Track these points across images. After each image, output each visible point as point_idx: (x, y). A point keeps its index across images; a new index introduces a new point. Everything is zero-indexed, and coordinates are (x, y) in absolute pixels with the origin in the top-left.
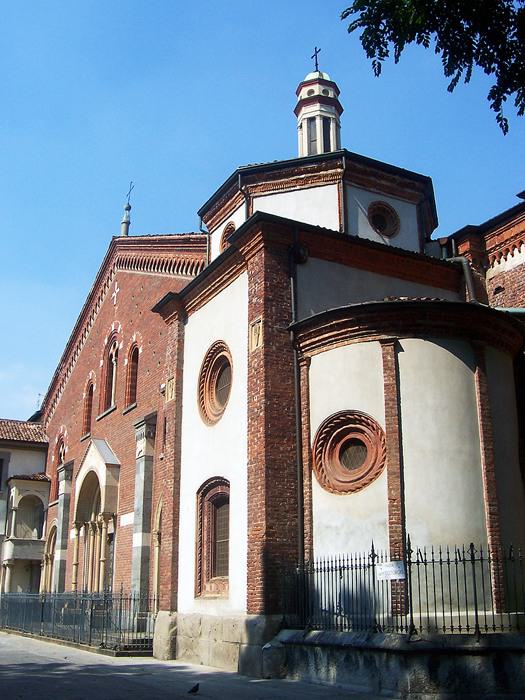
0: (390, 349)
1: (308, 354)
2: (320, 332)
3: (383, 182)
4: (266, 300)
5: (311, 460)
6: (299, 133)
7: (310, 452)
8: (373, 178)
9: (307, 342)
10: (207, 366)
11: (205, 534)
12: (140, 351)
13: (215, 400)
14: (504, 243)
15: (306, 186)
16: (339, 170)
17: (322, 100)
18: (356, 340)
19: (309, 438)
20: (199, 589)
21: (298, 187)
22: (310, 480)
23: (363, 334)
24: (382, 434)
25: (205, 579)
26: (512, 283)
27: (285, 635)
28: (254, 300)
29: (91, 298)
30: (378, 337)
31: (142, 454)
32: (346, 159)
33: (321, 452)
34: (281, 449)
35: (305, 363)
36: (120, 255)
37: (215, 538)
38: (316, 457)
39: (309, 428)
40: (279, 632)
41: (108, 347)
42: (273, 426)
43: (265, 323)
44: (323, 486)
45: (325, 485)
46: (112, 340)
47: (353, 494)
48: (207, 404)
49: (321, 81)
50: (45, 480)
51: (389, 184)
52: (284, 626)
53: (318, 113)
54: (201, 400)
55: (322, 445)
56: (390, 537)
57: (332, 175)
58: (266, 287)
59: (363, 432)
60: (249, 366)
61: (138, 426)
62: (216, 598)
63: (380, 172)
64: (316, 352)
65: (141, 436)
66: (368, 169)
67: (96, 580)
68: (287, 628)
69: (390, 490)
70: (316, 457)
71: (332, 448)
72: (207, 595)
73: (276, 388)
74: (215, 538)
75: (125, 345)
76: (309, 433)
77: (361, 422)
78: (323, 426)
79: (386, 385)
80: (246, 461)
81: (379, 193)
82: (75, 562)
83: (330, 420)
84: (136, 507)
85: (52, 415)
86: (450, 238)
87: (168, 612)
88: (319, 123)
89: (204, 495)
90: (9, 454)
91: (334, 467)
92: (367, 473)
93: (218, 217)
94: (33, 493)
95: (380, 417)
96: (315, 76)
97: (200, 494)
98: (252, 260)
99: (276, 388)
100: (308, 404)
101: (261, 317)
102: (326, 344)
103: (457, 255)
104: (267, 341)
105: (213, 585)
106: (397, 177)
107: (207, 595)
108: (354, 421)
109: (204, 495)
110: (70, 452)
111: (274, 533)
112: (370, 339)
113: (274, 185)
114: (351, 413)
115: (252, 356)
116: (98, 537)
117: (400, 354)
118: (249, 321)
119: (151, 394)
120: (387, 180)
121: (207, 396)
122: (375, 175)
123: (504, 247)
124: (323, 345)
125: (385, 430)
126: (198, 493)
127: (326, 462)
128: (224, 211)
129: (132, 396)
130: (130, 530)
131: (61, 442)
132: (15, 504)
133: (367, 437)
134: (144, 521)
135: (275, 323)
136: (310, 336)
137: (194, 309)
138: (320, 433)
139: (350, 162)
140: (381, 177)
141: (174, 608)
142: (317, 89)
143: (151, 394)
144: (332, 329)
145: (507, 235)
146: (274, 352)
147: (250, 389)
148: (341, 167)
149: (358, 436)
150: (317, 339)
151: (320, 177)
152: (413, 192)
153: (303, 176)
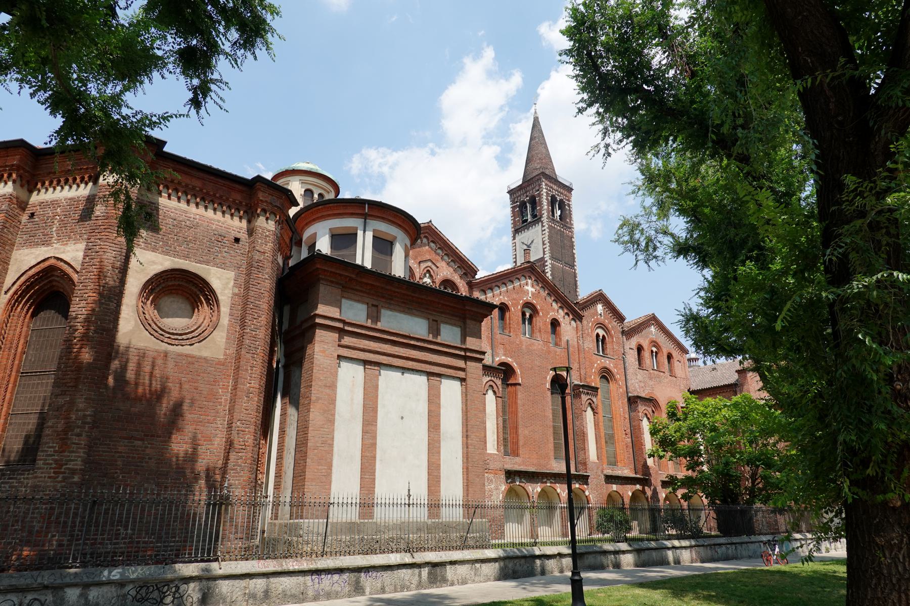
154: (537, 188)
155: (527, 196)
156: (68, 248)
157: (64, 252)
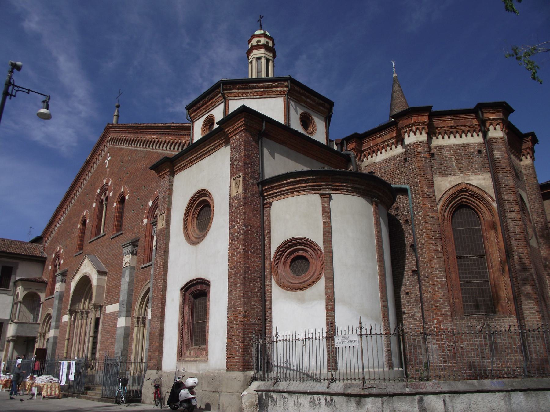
0: (326, 200)
1: (270, 200)
2: (281, 186)
3: (308, 100)
4: (245, 163)
5: (271, 268)
6: (250, 66)
7: (271, 263)
8: (303, 97)
9: (271, 192)
10: (191, 206)
11: (186, 317)
12: (127, 198)
13: (196, 228)
14: (376, 145)
15: (264, 96)
16: (285, 89)
17: (266, 47)
18: (305, 193)
19: (270, 254)
20: (181, 355)
21: (258, 97)
22: (271, 282)
23: (310, 190)
24: (321, 252)
25: (185, 348)
26: (380, 169)
27: (255, 385)
28: (236, 163)
29: (88, 163)
30: (319, 192)
31: (127, 265)
32: (290, 82)
33: (277, 263)
34: (253, 260)
35: (268, 205)
36: (111, 136)
37: (193, 319)
38: (275, 266)
39: (270, 248)
40: (251, 383)
41: (100, 195)
42: (248, 245)
43: (244, 178)
44: (280, 285)
45: (282, 285)
46: (104, 190)
47: (302, 292)
48: (190, 231)
49: (265, 35)
50: (43, 282)
51: (311, 102)
52: (254, 379)
53: (263, 55)
54: (186, 228)
55: (279, 259)
56: (327, 319)
57: (281, 91)
58: (245, 155)
59: (306, 251)
60: (230, 205)
61: (125, 246)
62: (196, 361)
63: (307, 94)
64: (276, 199)
65: (127, 253)
66: (301, 91)
67: (82, 350)
68: (256, 380)
69: (326, 288)
70: (275, 266)
71: (286, 261)
72: (187, 359)
73: (250, 220)
74: (193, 319)
75: (114, 194)
76: (270, 252)
77: (306, 245)
78: (281, 247)
79: (324, 222)
80: (227, 268)
81: (306, 107)
82: (67, 337)
83: (285, 243)
84: (121, 299)
85: (50, 238)
86: (343, 140)
87: (155, 371)
88: (263, 61)
89: (186, 291)
90: (17, 265)
91: (285, 271)
92: (310, 278)
93: (200, 111)
94: (33, 290)
95: (320, 242)
96: (261, 32)
97: (183, 290)
98: (234, 137)
99: (250, 220)
100: (270, 232)
101: (242, 174)
102: (283, 194)
103: (346, 150)
104: (245, 189)
105: (192, 352)
106: (316, 99)
107: (187, 359)
108: (301, 244)
109: (186, 291)
110: (64, 263)
111: (248, 316)
112: (314, 192)
113: (243, 93)
114: (301, 239)
115: (233, 199)
116: (85, 321)
117: (332, 202)
118: (231, 176)
119: (134, 226)
120: (310, 99)
121: (190, 226)
122: (305, 96)
123: (375, 148)
124: (282, 195)
125: (323, 251)
126: (182, 289)
127: (281, 270)
128: (206, 107)
129: (119, 227)
130: (115, 316)
131: (57, 257)
132: (20, 298)
133: (310, 254)
134: (127, 310)
135: (250, 179)
136: (273, 188)
137: (181, 169)
138: (278, 251)
139: (292, 84)
140: (308, 97)
141: (159, 367)
142: (263, 40)
143: (134, 226)
144: (289, 184)
145: (379, 140)
146: (249, 197)
147: (231, 221)
148: (287, 86)
149: (304, 254)
150: (278, 191)
151: (273, 92)
152: (323, 109)
153: (262, 90)
156: (471, 178)
157: (469, 180)
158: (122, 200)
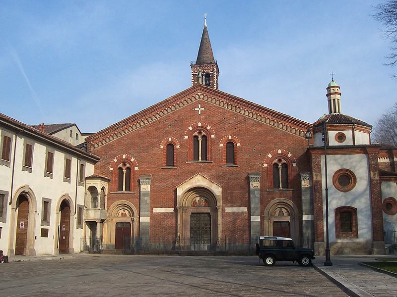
154: (211, 70)
155: (204, 72)
158: (230, 145)
